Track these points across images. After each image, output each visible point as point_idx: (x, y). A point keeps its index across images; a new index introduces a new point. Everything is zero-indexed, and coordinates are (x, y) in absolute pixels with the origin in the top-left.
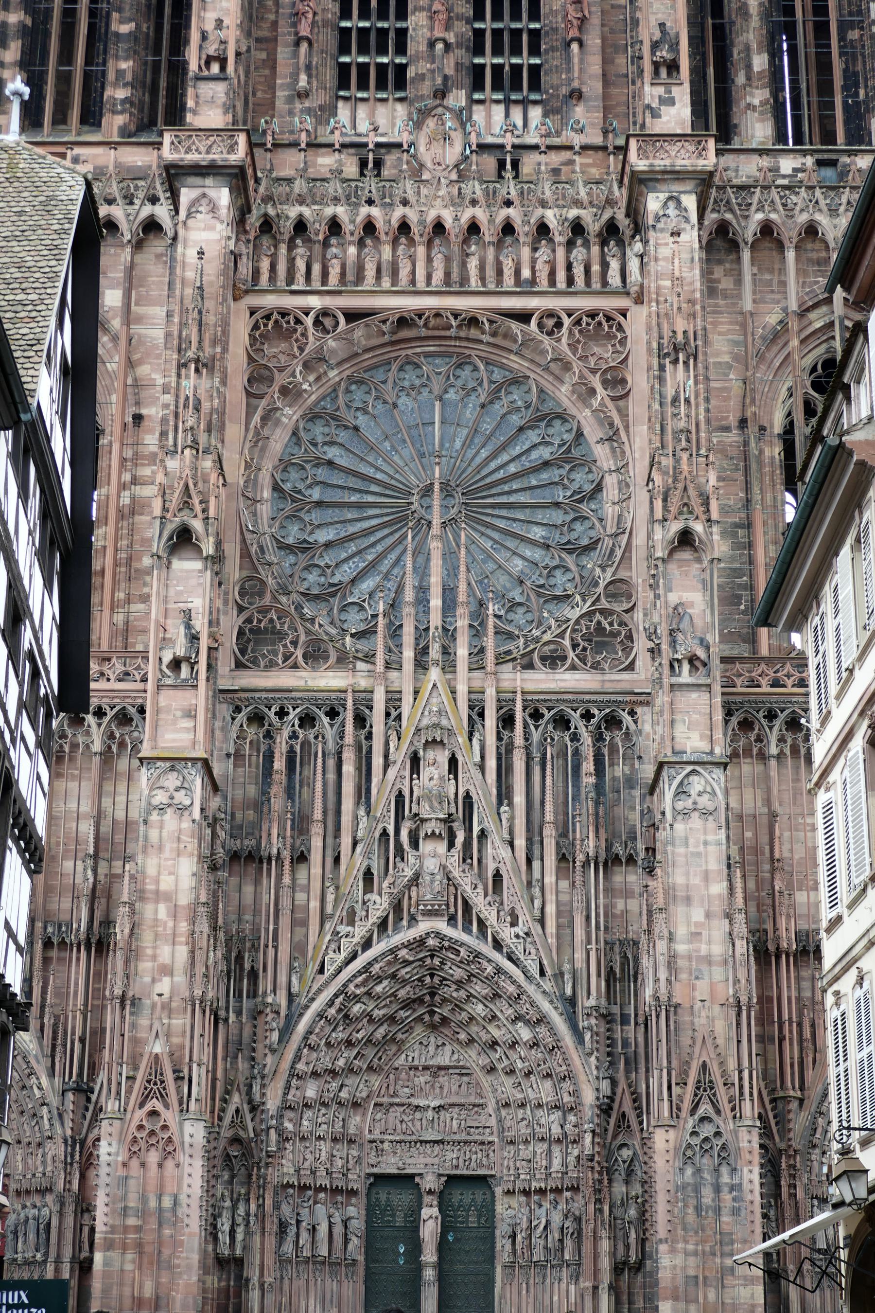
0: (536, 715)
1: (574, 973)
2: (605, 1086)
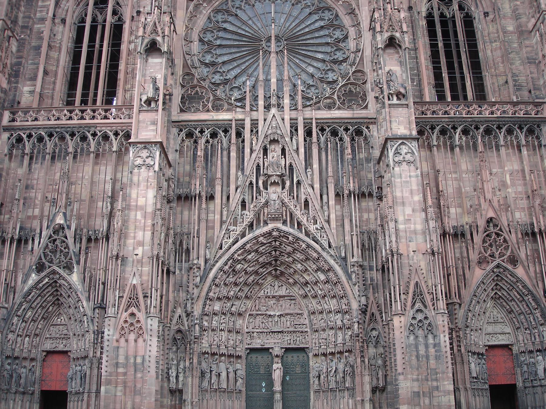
0: (322, 130)
1: (345, 246)
2: (363, 300)
